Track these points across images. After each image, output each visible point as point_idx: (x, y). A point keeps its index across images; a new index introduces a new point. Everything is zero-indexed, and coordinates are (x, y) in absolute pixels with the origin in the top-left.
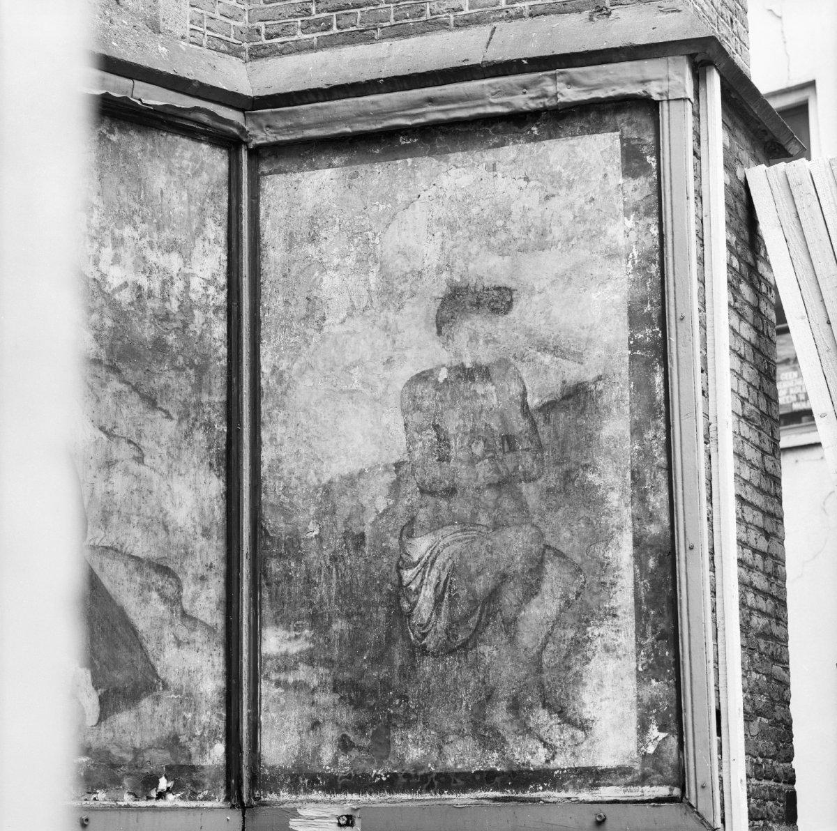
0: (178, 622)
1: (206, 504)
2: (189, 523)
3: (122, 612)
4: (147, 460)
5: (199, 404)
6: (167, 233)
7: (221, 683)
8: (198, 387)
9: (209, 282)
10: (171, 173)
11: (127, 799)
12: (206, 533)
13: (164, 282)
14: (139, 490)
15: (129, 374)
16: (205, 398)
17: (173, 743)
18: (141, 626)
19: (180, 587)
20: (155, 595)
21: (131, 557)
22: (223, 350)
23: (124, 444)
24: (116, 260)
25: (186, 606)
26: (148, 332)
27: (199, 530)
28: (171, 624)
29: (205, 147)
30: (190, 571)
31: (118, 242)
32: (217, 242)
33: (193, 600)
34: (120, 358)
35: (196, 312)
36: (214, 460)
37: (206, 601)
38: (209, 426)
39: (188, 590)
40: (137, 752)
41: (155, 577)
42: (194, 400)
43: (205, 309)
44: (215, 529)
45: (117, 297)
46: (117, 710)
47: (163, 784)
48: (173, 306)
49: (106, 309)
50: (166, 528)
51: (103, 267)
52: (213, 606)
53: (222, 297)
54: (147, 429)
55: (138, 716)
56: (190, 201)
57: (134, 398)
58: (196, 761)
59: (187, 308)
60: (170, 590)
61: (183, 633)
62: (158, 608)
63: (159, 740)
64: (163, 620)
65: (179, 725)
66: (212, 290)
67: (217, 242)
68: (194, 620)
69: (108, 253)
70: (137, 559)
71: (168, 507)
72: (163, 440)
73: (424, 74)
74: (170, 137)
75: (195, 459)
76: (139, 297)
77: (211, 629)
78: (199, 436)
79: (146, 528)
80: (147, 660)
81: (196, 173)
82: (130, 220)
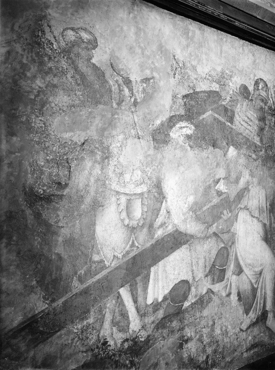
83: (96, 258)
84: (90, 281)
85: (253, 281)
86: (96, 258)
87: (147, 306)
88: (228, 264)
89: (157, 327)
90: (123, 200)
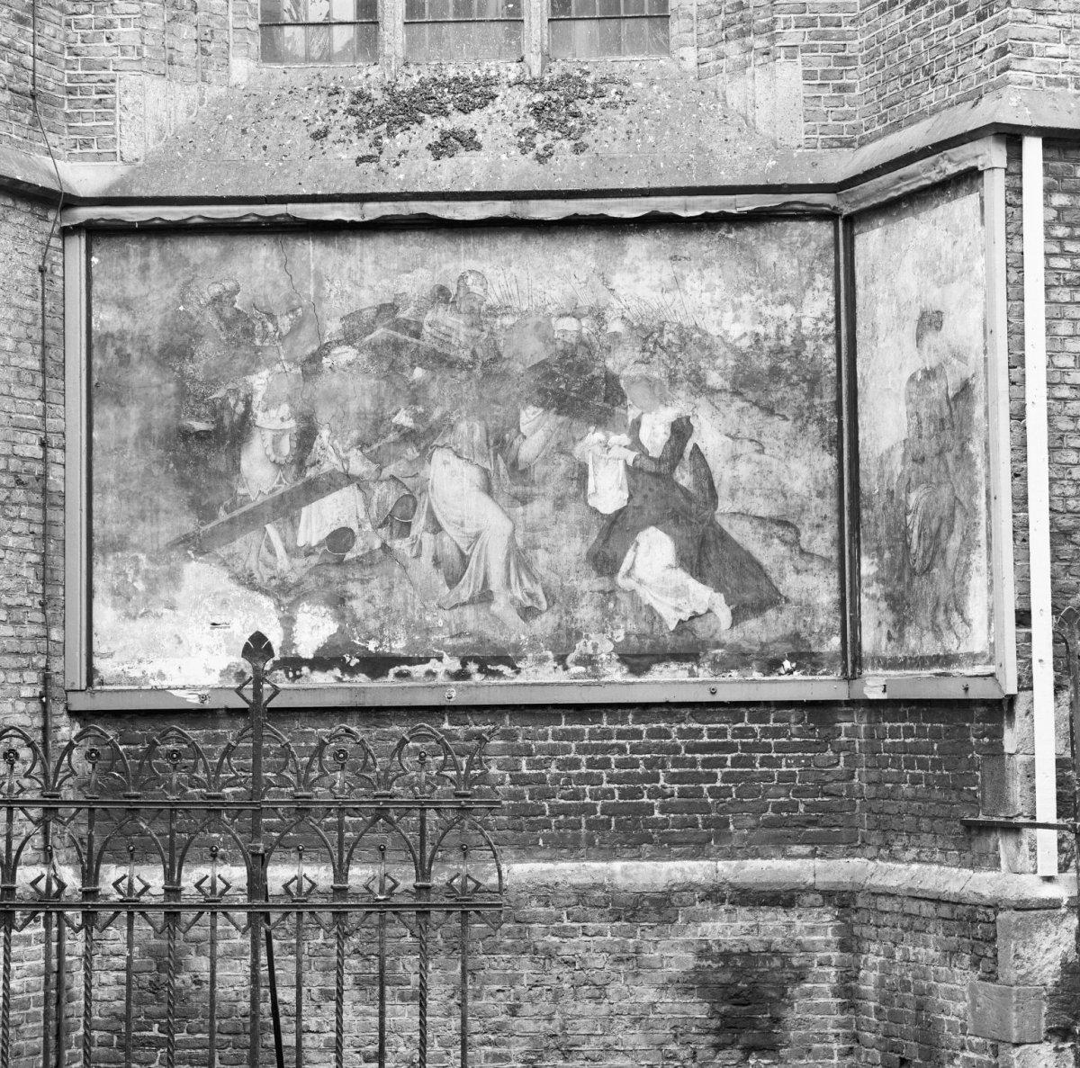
0: (797, 558)
1: (820, 475)
2: (805, 490)
3: (748, 554)
4: (767, 451)
5: (812, 406)
6: (780, 292)
7: (836, 596)
8: (811, 394)
9: (818, 319)
10: (782, 249)
11: (757, 675)
12: (821, 495)
13: (779, 327)
14: (761, 472)
15: (750, 395)
16: (817, 401)
17: (796, 637)
18: (765, 562)
19: (798, 533)
20: (776, 541)
21: (756, 517)
22: (834, 365)
23: (747, 443)
24: (736, 319)
25: (804, 545)
26: (764, 364)
27: (814, 493)
28: (791, 559)
29: (812, 224)
30: (807, 522)
31: (737, 307)
32: (825, 289)
33: (810, 542)
34: (741, 385)
35: (808, 343)
36: (826, 444)
37: (822, 542)
38: (821, 420)
39: (805, 535)
40: (763, 645)
41: (776, 529)
42: (807, 404)
43: (816, 338)
44: (828, 491)
45: (738, 344)
46: (746, 618)
47: (787, 664)
48: (788, 341)
49: (729, 355)
50: (784, 495)
51: (725, 326)
52: (828, 544)
53: (832, 327)
54: (767, 430)
55: (764, 621)
56: (800, 265)
57: (755, 410)
58: (815, 649)
59: (799, 342)
60: (790, 536)
61: (802, 564)
62: (778, 548)
63: (782, 637)
64: (784, 557)
65: (800, 626)
66: (821, 324)
67: (825, 289)
68: (812, 555)
69: (729, 315)
70: (761, 518)
71: (785, 480)
72: (780, 436)
73: (877, 167)
74: (780, 224)
75: (809, 445)
76: (757, 341)
77: (827, 560)
78: (813, 428)
79: (767, 497)
80: (770, 583)
81: (804, 244)
82: (748, 289)
83: (241, 491)
84: (236, 513)
85: (463, 546)
86: (241, 491)
87: (297, 547)
88: (416, 516)
89: (310, 573)
90: (269, 436)
